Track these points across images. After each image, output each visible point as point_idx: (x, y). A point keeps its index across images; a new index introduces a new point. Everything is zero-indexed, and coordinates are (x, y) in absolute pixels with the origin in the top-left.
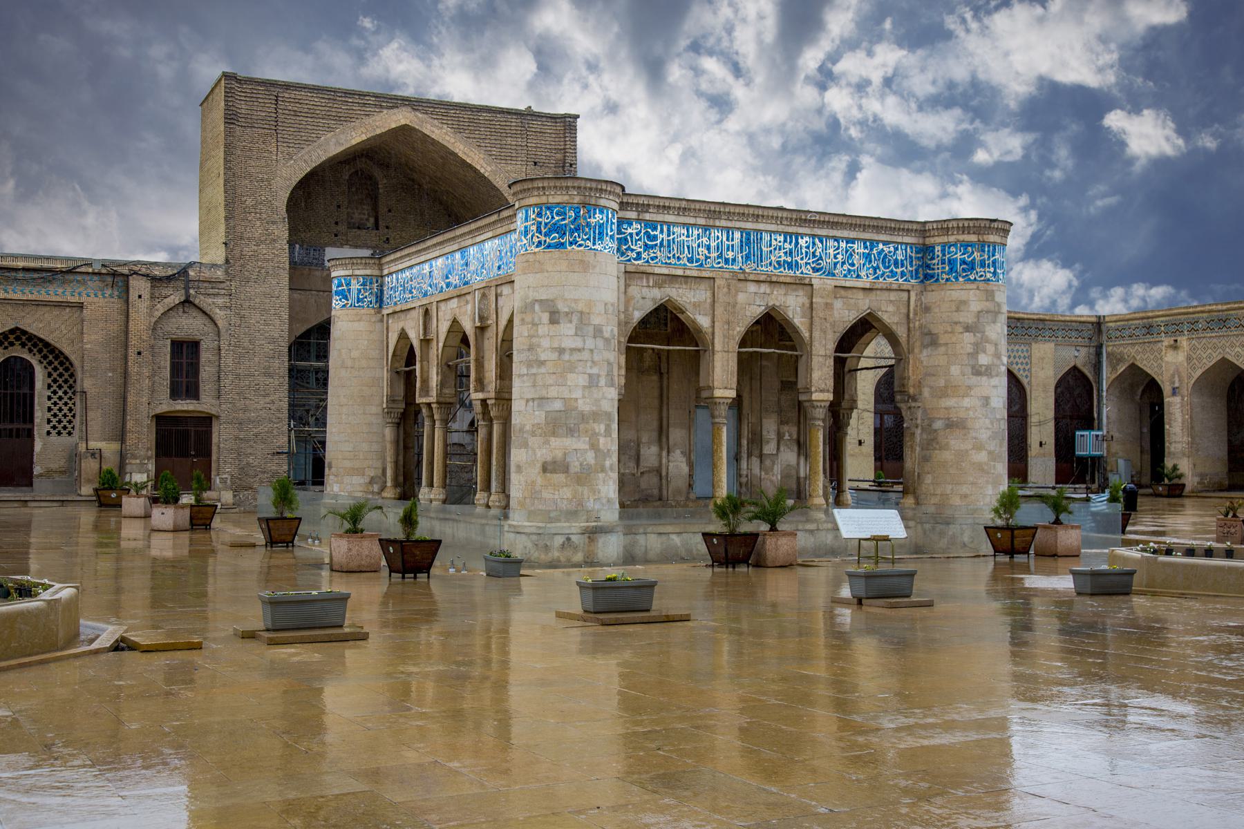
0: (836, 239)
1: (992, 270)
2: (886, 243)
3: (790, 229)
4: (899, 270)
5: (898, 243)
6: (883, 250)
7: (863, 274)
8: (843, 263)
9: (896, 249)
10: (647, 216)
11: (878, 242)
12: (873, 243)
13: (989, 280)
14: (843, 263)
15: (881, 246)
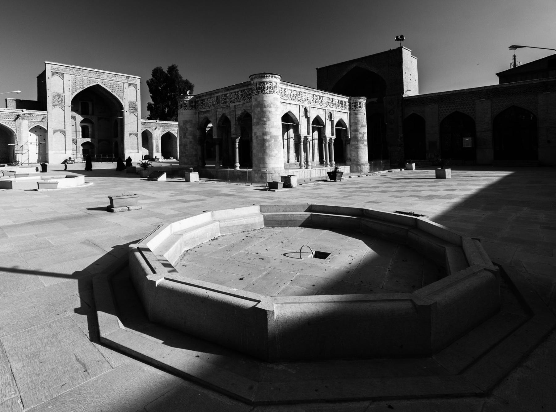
0: (235, 92)
1: (256, 91)
2: (246, 90)
3: (225, 93)
4: (250, 97)
5: (249, 89)
6: (246, 92)
7: (241, 100)
8: (237, 98)
9: (249, 90)
10: (201, 99)
11: (245, 90)
12: (244, 90)
13: (255, 95)
14: (237, 98)
15: (245, 91)
